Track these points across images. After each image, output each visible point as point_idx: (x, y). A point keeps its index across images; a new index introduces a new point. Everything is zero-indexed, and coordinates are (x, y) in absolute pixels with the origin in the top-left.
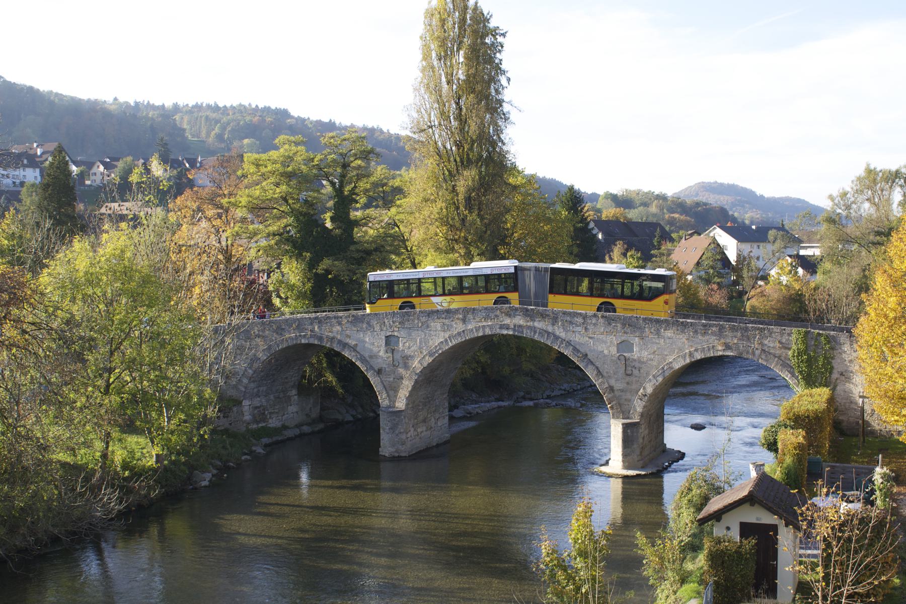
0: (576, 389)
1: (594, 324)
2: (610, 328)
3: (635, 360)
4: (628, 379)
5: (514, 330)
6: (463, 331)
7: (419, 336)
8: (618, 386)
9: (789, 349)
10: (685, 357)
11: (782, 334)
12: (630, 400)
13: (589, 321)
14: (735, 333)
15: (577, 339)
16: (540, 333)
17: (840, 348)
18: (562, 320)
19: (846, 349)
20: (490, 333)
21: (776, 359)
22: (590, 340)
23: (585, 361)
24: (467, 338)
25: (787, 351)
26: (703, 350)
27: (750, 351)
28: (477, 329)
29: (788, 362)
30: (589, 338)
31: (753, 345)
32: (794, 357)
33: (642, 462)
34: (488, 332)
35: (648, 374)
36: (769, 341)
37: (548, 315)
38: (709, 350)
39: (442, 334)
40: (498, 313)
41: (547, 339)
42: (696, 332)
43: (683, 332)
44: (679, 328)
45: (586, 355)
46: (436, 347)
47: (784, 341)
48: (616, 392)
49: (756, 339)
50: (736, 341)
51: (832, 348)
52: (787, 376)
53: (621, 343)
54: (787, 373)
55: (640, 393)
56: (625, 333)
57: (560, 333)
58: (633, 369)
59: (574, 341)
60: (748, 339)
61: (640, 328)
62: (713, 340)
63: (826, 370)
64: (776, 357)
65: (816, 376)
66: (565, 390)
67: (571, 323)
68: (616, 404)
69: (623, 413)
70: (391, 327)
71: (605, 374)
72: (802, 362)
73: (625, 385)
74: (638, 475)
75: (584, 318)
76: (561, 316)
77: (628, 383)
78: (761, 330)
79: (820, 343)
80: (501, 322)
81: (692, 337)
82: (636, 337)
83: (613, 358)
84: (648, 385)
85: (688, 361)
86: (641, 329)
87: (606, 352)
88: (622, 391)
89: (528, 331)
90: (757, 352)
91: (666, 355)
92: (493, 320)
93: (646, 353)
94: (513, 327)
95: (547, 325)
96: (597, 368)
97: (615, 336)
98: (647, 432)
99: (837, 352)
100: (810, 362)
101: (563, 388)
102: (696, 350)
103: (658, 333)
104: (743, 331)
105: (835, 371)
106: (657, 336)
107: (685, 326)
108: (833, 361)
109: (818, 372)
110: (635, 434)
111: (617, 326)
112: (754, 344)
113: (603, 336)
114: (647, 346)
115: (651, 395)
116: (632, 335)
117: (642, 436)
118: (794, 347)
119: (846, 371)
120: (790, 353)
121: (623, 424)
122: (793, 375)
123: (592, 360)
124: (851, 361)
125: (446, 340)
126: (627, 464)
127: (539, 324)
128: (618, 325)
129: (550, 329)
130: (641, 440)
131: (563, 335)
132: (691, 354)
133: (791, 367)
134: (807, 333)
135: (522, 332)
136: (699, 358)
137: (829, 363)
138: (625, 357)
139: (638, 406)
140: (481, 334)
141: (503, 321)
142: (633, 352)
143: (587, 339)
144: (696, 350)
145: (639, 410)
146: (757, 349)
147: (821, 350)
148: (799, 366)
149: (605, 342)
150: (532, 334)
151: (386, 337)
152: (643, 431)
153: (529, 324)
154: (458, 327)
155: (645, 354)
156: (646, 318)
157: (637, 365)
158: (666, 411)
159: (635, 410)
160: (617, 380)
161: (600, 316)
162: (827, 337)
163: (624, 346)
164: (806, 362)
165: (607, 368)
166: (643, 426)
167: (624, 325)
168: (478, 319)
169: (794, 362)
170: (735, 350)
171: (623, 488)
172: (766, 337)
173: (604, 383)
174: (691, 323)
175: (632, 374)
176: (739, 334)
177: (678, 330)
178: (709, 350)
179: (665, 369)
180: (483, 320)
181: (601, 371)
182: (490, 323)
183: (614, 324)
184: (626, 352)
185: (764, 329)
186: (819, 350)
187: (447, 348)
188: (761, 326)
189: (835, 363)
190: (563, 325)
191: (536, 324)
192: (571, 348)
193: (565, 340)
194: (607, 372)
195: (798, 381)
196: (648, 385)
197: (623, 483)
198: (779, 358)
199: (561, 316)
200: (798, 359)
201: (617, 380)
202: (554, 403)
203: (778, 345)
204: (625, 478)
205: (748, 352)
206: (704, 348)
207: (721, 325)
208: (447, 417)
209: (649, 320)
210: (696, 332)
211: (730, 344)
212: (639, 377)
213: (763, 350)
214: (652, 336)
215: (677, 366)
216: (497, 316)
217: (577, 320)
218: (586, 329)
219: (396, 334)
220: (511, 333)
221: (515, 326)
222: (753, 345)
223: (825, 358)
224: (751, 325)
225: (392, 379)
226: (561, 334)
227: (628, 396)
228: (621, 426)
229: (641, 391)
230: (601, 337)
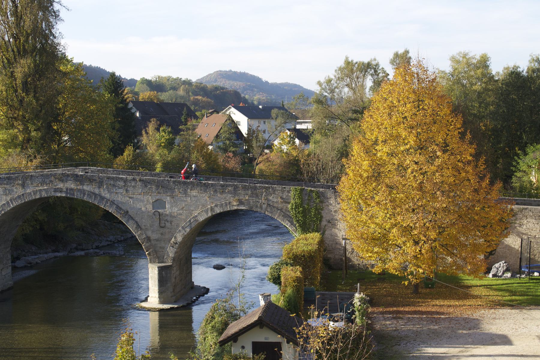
0: (120, 240)
1: (134, 187)
2: (146, 190)
3: (167, 215)
4: (162, 230)
5: (66, 193)
6: (23, 195)
9: (289, 203)
10: (207, 212)
11: (283, 192)
12: (163, 248)
13: (129, 184)
14: (247, 192)
15: (119, 199)
16: (88, 195)
17: (328, 202)
18: (107, 184)
19: (332, 202)
20: (46, 196)
21: (279, 211)
22: (130, 200)
23: (127, 216)
24: (26, 200)
25: (287, 205)
26: (222, 205)
27: (259, 206)
28: (35, 193)
29: (288, 213)
30: (130, 198)
31: (260, 201)
32: (292, 209)
34: (44, 195)
35: (178, 226)
36: (273, 197)
37: (95, 180)
38: (226, 205)
39: (4, 197)
41: (95, 199)
42: (215, 191)
43: (205, 191)
44: (202, 188)
45: (127, 212)
47: (284, 197)
48: (152, 242)
49: (263, 196)
50: (247, 198)
51: (321, 202)
52: (287, 225)
53: (156, 201)
54: (287, 222)
55: (172, 242)
56: (159, 193)
57: (105, 194)
58: (166, 223)
59: (117, 200)
60: (257, 196)
61: (171, 189)
62: (229, 197)
63: (317, 219)
64: (279, 209)
65: (309, 224)
66: (111, 241)
67: (114, 186)
68: (152, 251)
69: (158, 258)
71: (143, 227)
72: (298, 213)
73: (160, 235)
74: (172, 309)
75: (125, 182)
76: (106, 181)
77: (162, 234)
78: (267, 188)
79: (312, 198)
80: (55, 186)
81: (213, 195)
82: (168, 196)
83: (150, 214)
84: (178, 235)
85: (210, 214)
86: (172, 190)
87: (143, 209)
88: (157, 240)
89: (79, 193)
90: (264, 206)
91: (193, 210)
92: (48, 185)
93: (176, 209)
94: (65, 190)
95: (94, 188)
96: (137, 222)
97: (150, 195)
98: (178, 273)
99: (325, 204)
100: (305, 213)
101: (109, 239)
102: (216, 206)
103: (185, 193)
104: (253, 190)
105: (324, 220)
106: (185, 195)
107: (207, 187)
108: (322, 212)
109: (311, 221)
110: (169, 275)
111: (152, 188)
112: (261, 199)
113: (141, 196)
114: (177, 203)
115: (181, 243)
116: (164, 195)
117: (174, 276)
118: (292, 201)
119: (332, 219)
120: (289, 206)
121: (158, 267)
122: (292, 223)
123: (132, 216)
124: (335, 211)
125: (8, 203)
126: (162, 299)
127: (87, 188)
128: (153, 187)
129: (97, 191)
130: (173, 280)
131: (107, 196)
132: (212, 209)
133: (291, 218)
134: (302, 190)
135: (74, 195)
136: (218, 212)
137: (320, 213)
138: (159, 212)
139: (171, 252)
140: (38, 197)
141: (57, 185)
143: (128, 199)
144: (216, 206)
145: (171, 255)
146: (264, 204)
147: (313, 204)
148: (296, 217)
149: (143, 201)
150: (82, 195)
152: (175, 272)
153: (79, 187)
154: (19, 191)
155: (175, 210)
156: (175, 181)
157: (169, 219)
158: (193, 255)
159: (168, 256)
160: (153, 232)
161: (138, 179)
162: (317, 193)
163: (159, 204)
164: (302, 213)
166: (175, 268)
167: (158, 187)
168: (35, 184)
169: (292, 213)
170: (247, 205)
171: (159, 319)
172: (270, 194)
173: (143, 234)
174: (212, 184)
175: (165, 226)
176: (250, 192)
177: (201, 190)
178: (226, 205)
179: (192, 221)
180: (40, 185)
181: (140, 224)
182: (45, 188)
183: (149, 186)
184: (159, 209)
185: (269, 187)
186: (312, 204)
187: (9, 209)
188: (267, 185)
189: (324, 213)
190: (107, 188)
191: (85, 187)
192: (115, 206)
193: (109, 200)
194: (145, 225)
195: (296, 228)
196: (178, 235)
198: (281, 210)
199: (106, 181)
200: (296, 211)
201: (153, 232)
202: (102, 252)
203: (280, 200)
204: (161, 311)
205: (257, 207)
206: (222, 204)
207: (236, 185)
208: (10, 268)
209: (178, 183)
210: (215, 191)
211: (243, 200)
212: (171, 229)
213: (269, 205)
214: (181, 195)
215: (201, 219)
216: (51, 181)
217: (119, 183)
218: (127, 191)
220: (64, 195)
221: (67, 189)
222: (260, 201)
223: (316, 209)
224: (258, 185)
226: (106, 195)
228: (157, 269)
229: (173, 240)
230: (139, 197)
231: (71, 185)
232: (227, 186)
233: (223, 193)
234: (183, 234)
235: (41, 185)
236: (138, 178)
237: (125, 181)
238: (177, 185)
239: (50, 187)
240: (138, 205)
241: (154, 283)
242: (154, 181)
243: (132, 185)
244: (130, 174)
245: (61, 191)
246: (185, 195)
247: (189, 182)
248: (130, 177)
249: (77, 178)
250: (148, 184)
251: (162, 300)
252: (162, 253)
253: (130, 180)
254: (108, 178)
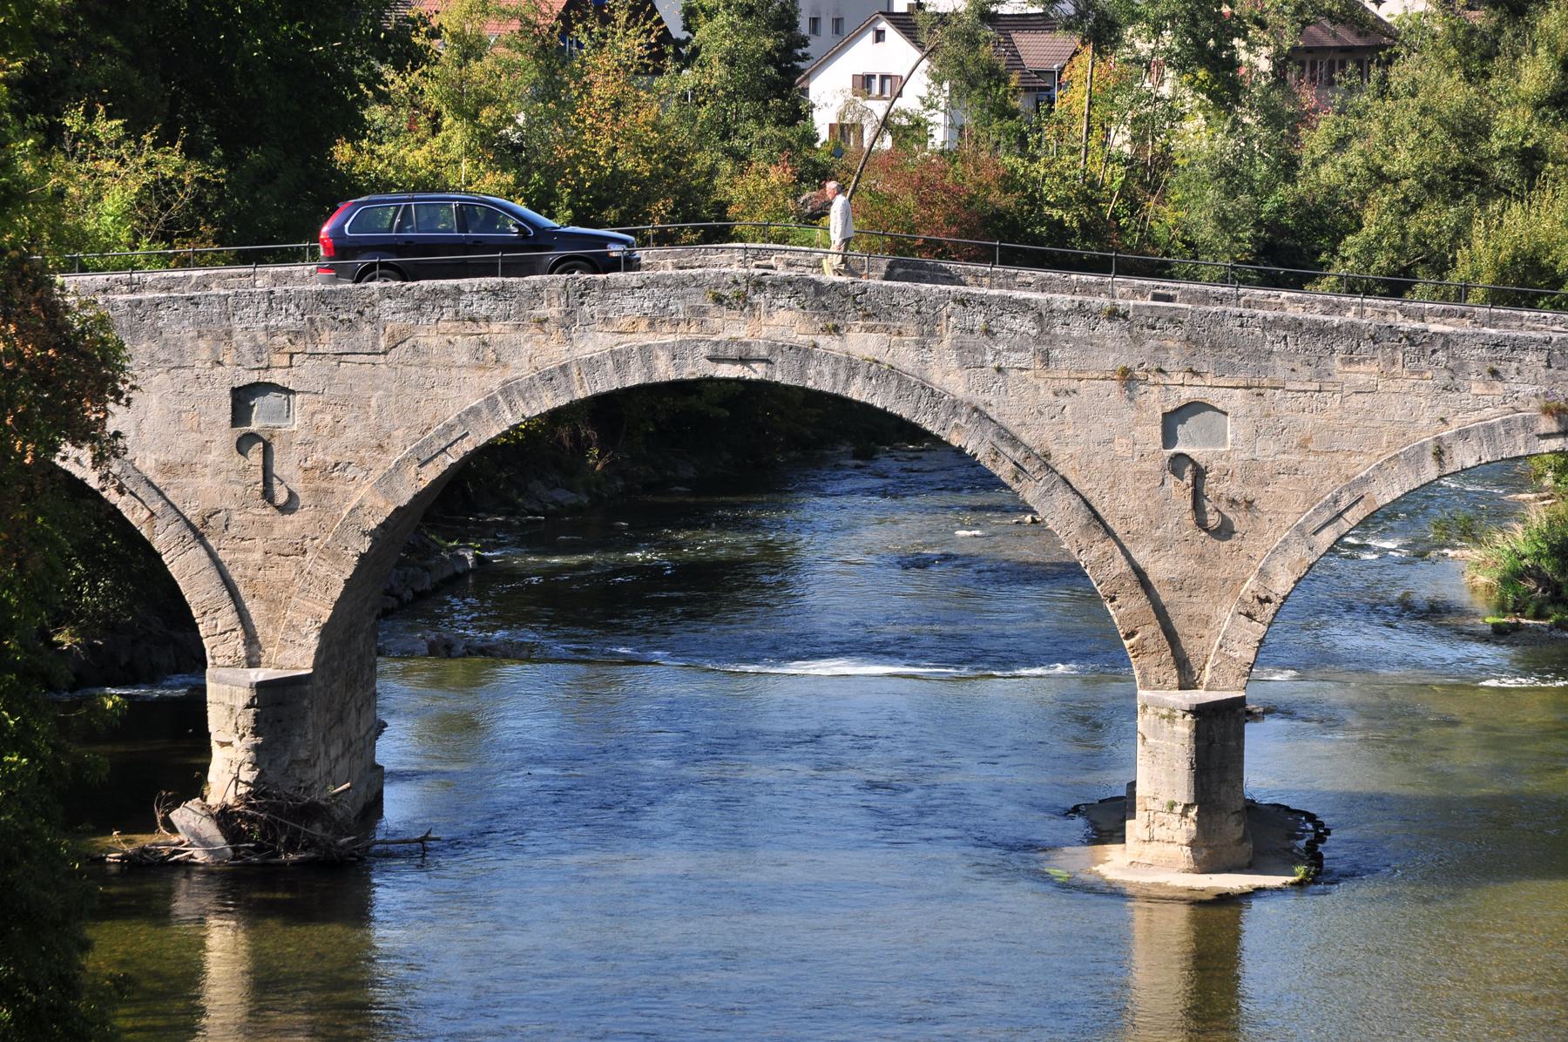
0: (418, 589)
7: (377, 388)
28: (620, 359)
33: (1249, 846)
34: (664, 371)
39: (474, 377)
46: (450, 428)
70: (258, 350)
92: (683, 327)
111: (1166, 350)
123: (1072, 478)
125: (492, 402)
126: (1205, 852)
127: (861, 342)
128: (1170, 344)
140: (635, 378)
142: (1224, 444)
151: (234, 391)
165: (1117, 506)
168: (625, 323)
182: (670, 339)
183: (1153, 343)
187: (494, 432)
197: (1194, 920)
201: (1161, 546)
209: (1287, 328)
218: (1046, 360)
219: (277, 377)
225: (258, 556)
227: (1201, 603)
234: (1301, 560)
235: (651, 324)
237: (1043, 317)
238: (1285, 337)
239: (694, 337)
241: (1163, 777)
243: (1075, 334)
244: (970, 279)
246: (1315, 386)
247: (1339, 326)
248: (1062, 300)
250: (1146, 331)
252: (1195, 641)
253: (1066, 314)
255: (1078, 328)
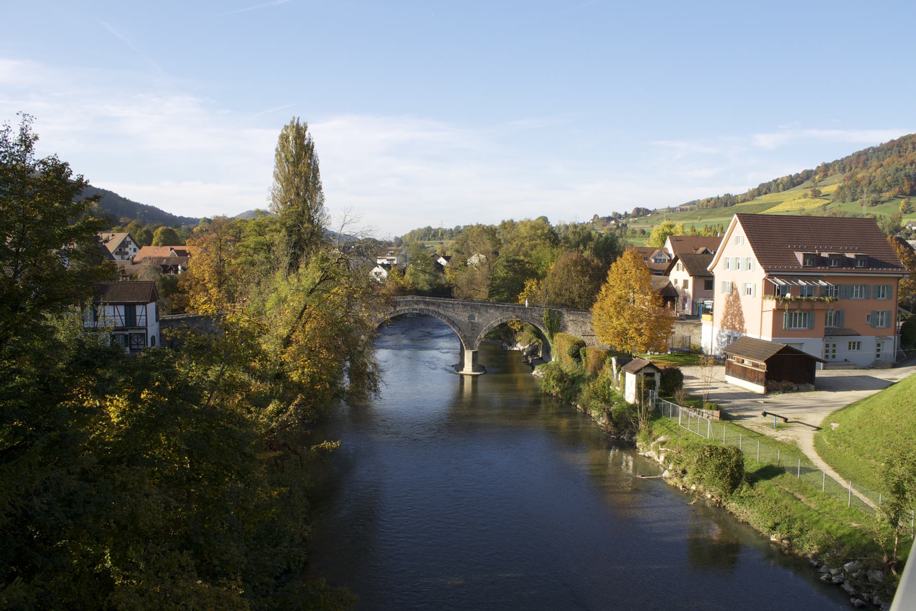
1: (458, 308)
2: (465, 309)
4: (473, 331)
5: (419, 310)
8: (468, 335)
26: (506, 318)
28: (401, 311)
34: (406, 312)
40: (411, 303)
42: (503, 310)
43: (498, 310)
51: (560, 316)
60: (526, 313)
62: (510, 314)
67: (447, 307)
85: (500, 323)
86: (479, 309)
88: (470, 337)
100: (551, 322)
103: (487, 311)
118: (545, 316)
120: (543, 319)
122: (544, 327)
129: (437, 310)
131: (443, 313)
132: (501, 320)
134: (550, 310)
139: (477, 343)
145: (478, 345)
155: (481, 320)
157: (477, 325)
162: (558, 311)
163: (471, 317)
167: (471, 308)
176: (522, 311)
190: (443, 308)
191: (430, 308)
203: (538, 315)
210: (503, 310)
213: (532, 318)
215: (495, 326)
231: (422, 306)
232: (510, 307)
233: (507, 311)
236: (460, 303)
237: (453, 304)
240: (460, 318)
242: (469, 304)
245: (416, 310)
249: (425, 303)
251: (474, 370)
254: (444, 303)
255: (457, 306)
